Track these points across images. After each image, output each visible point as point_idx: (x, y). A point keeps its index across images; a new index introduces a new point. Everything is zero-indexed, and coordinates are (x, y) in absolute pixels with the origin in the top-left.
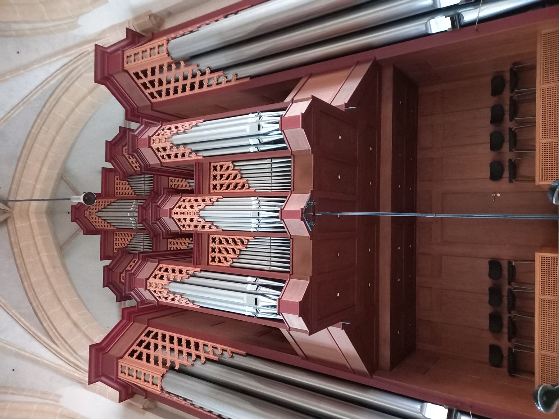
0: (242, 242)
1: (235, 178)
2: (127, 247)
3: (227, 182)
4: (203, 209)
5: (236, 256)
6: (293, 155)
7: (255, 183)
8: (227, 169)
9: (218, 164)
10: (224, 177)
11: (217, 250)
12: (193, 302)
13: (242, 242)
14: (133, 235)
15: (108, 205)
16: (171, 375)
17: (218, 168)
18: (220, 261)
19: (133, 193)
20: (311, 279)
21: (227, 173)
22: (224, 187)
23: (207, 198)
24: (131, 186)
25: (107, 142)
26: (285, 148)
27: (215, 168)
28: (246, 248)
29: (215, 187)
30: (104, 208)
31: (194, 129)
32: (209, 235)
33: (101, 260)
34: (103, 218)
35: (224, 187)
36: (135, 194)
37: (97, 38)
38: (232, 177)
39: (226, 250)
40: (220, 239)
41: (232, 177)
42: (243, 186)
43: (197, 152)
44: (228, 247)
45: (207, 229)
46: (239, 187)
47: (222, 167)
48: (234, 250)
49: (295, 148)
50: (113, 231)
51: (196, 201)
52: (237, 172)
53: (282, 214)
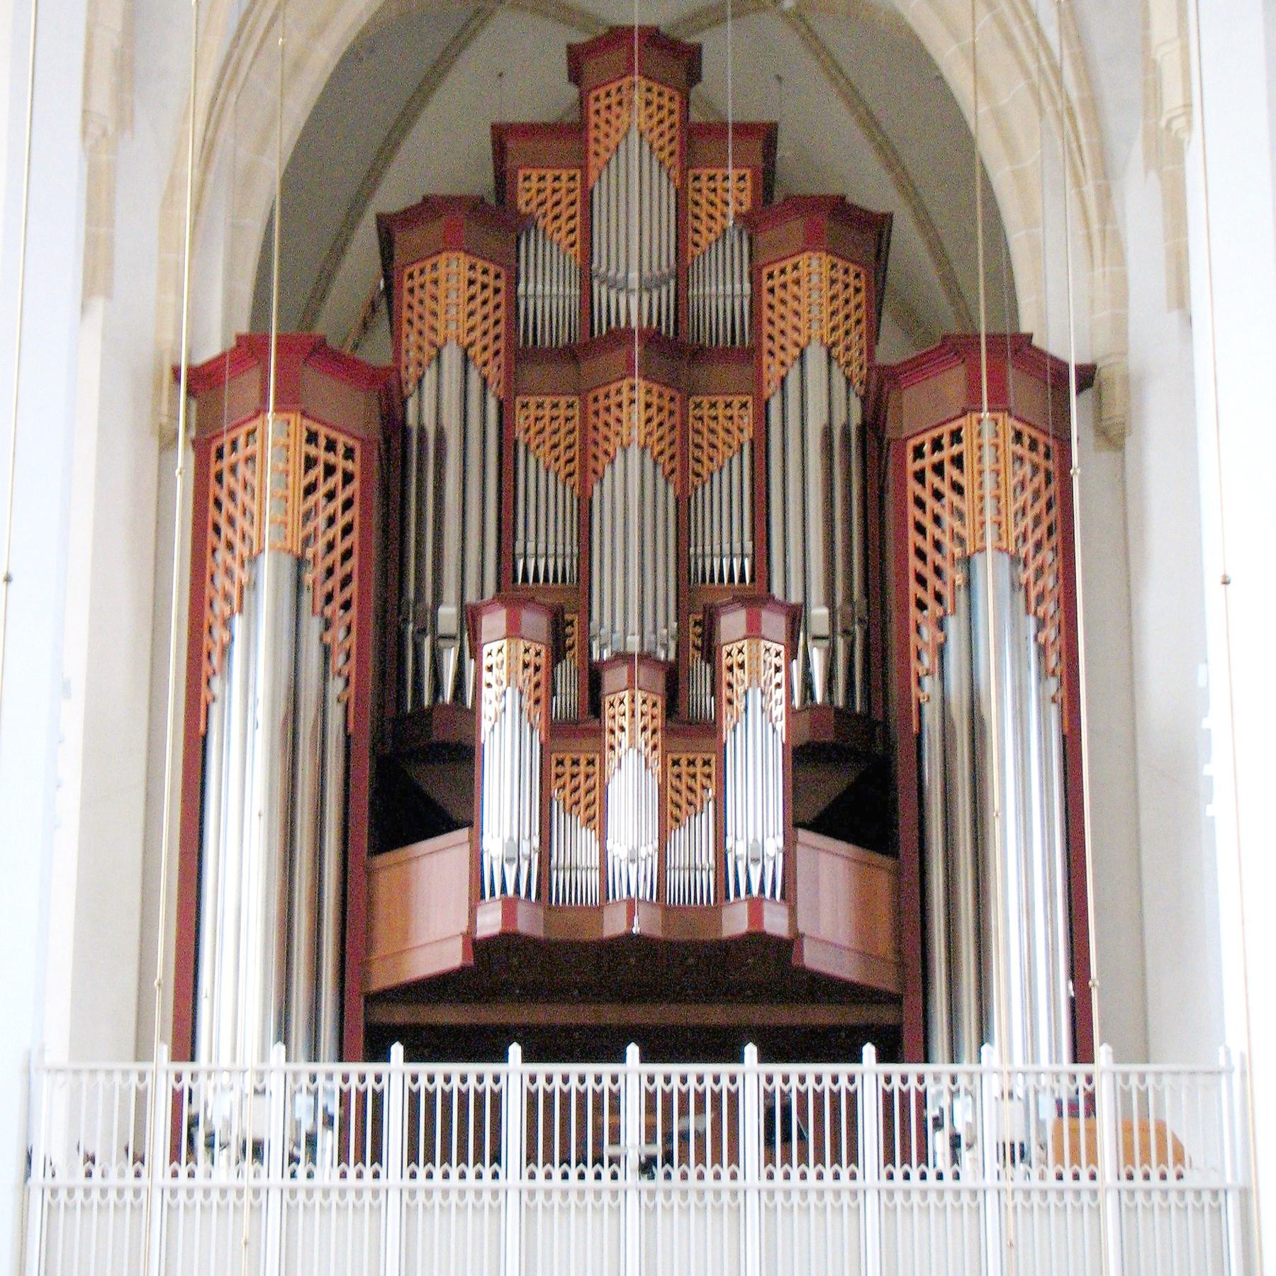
0: (589, 820)
1: (690, 803)
2: (536, 227)
3: (683, 788)
4: (639, 751)
5: (568, 807)
6: (717, 909)
7: (679, 838)
8: (703, 787)
9: (713, 770)
10: (691, 782)
11: (575, 770)
12: (493, 729)
13: (589, 820)
14: (572, 251)
15: (661, 163)
16: (288, 563)
17: (706, 770)
18: (558, 776)
19: (698, 252)
20: (547, 941)
21: (698, 788)
22: (676, 782)
23: (658, 753)
24: (717, 241)
25: (843, 198)
26: (728, 897)
27: (706, 763)
28: (581, 828)
29: (676, 763)
30: (651, 153)
31: (770, 726)
32: (599, 752)
33: (493, 127)
34: (622, 148)
35: (676, 782)
36: (693, 257)
37: (1109, 227)
38: (691, 797)
39: (575, 790)
40: (594, 774)
41: (691, 797)
42: (677, 820)
43: (735, 730)
44: (582, 791)
45: (608, 754)
46: (676, 812)
47: (709, 776)
48: (577, 803)
49: (726, 912)
50: (584, 168)
51: (654, 732)
52: (698, 808)
53: (631, 904)
